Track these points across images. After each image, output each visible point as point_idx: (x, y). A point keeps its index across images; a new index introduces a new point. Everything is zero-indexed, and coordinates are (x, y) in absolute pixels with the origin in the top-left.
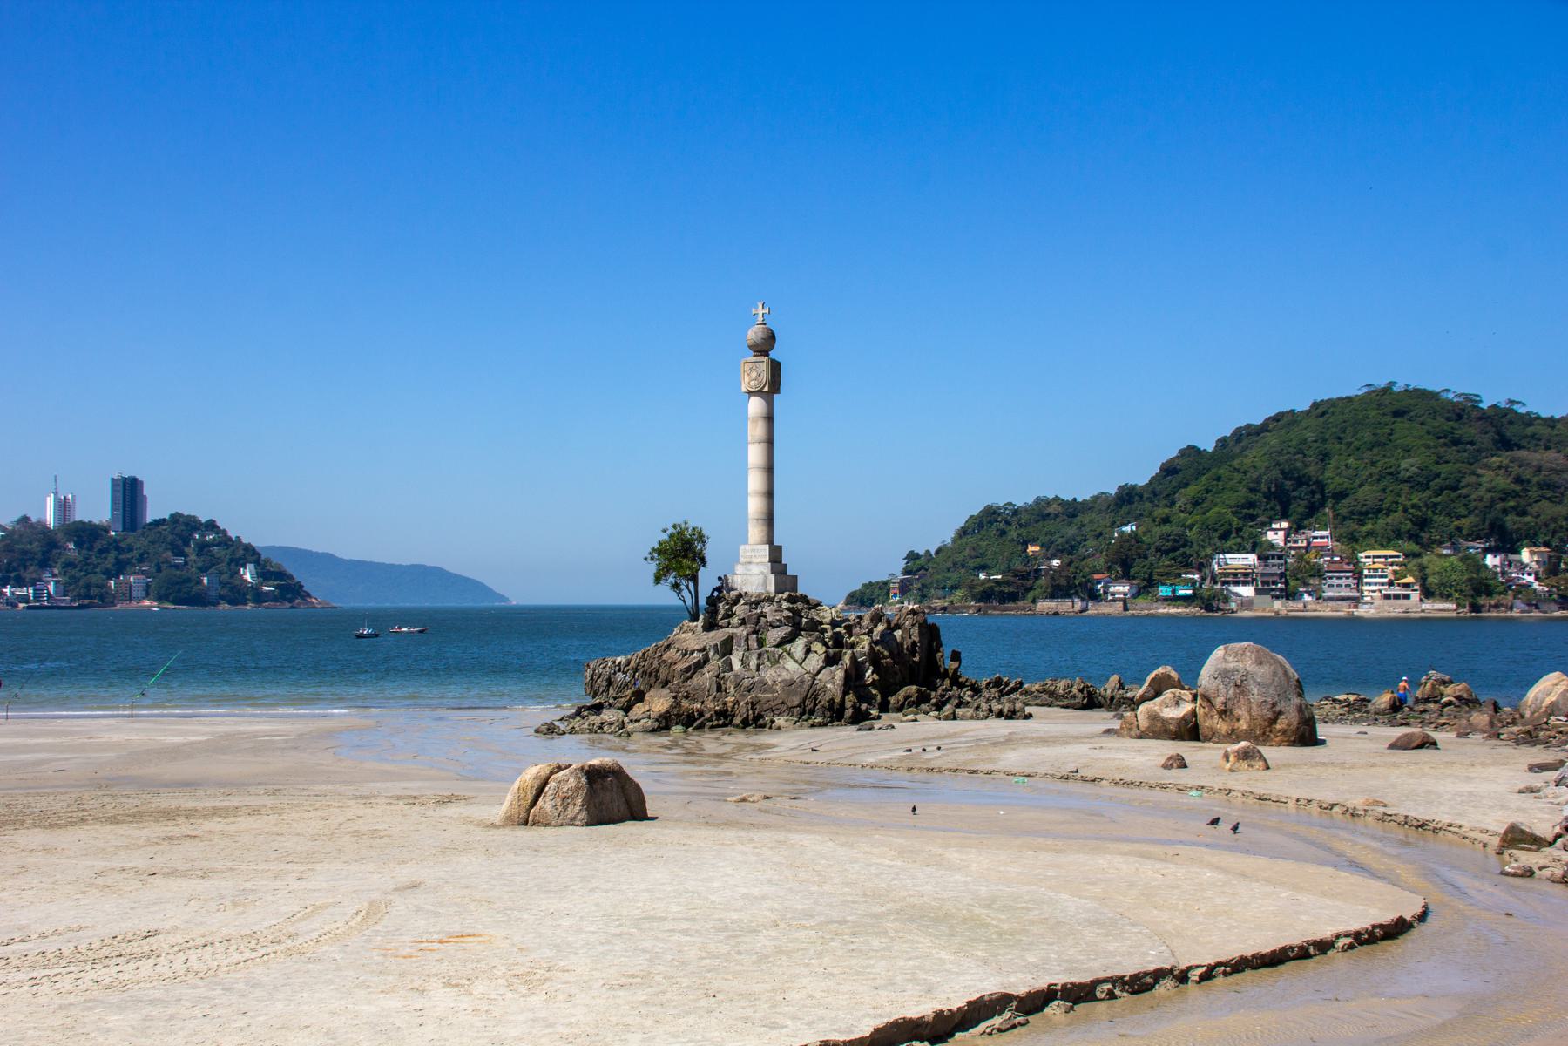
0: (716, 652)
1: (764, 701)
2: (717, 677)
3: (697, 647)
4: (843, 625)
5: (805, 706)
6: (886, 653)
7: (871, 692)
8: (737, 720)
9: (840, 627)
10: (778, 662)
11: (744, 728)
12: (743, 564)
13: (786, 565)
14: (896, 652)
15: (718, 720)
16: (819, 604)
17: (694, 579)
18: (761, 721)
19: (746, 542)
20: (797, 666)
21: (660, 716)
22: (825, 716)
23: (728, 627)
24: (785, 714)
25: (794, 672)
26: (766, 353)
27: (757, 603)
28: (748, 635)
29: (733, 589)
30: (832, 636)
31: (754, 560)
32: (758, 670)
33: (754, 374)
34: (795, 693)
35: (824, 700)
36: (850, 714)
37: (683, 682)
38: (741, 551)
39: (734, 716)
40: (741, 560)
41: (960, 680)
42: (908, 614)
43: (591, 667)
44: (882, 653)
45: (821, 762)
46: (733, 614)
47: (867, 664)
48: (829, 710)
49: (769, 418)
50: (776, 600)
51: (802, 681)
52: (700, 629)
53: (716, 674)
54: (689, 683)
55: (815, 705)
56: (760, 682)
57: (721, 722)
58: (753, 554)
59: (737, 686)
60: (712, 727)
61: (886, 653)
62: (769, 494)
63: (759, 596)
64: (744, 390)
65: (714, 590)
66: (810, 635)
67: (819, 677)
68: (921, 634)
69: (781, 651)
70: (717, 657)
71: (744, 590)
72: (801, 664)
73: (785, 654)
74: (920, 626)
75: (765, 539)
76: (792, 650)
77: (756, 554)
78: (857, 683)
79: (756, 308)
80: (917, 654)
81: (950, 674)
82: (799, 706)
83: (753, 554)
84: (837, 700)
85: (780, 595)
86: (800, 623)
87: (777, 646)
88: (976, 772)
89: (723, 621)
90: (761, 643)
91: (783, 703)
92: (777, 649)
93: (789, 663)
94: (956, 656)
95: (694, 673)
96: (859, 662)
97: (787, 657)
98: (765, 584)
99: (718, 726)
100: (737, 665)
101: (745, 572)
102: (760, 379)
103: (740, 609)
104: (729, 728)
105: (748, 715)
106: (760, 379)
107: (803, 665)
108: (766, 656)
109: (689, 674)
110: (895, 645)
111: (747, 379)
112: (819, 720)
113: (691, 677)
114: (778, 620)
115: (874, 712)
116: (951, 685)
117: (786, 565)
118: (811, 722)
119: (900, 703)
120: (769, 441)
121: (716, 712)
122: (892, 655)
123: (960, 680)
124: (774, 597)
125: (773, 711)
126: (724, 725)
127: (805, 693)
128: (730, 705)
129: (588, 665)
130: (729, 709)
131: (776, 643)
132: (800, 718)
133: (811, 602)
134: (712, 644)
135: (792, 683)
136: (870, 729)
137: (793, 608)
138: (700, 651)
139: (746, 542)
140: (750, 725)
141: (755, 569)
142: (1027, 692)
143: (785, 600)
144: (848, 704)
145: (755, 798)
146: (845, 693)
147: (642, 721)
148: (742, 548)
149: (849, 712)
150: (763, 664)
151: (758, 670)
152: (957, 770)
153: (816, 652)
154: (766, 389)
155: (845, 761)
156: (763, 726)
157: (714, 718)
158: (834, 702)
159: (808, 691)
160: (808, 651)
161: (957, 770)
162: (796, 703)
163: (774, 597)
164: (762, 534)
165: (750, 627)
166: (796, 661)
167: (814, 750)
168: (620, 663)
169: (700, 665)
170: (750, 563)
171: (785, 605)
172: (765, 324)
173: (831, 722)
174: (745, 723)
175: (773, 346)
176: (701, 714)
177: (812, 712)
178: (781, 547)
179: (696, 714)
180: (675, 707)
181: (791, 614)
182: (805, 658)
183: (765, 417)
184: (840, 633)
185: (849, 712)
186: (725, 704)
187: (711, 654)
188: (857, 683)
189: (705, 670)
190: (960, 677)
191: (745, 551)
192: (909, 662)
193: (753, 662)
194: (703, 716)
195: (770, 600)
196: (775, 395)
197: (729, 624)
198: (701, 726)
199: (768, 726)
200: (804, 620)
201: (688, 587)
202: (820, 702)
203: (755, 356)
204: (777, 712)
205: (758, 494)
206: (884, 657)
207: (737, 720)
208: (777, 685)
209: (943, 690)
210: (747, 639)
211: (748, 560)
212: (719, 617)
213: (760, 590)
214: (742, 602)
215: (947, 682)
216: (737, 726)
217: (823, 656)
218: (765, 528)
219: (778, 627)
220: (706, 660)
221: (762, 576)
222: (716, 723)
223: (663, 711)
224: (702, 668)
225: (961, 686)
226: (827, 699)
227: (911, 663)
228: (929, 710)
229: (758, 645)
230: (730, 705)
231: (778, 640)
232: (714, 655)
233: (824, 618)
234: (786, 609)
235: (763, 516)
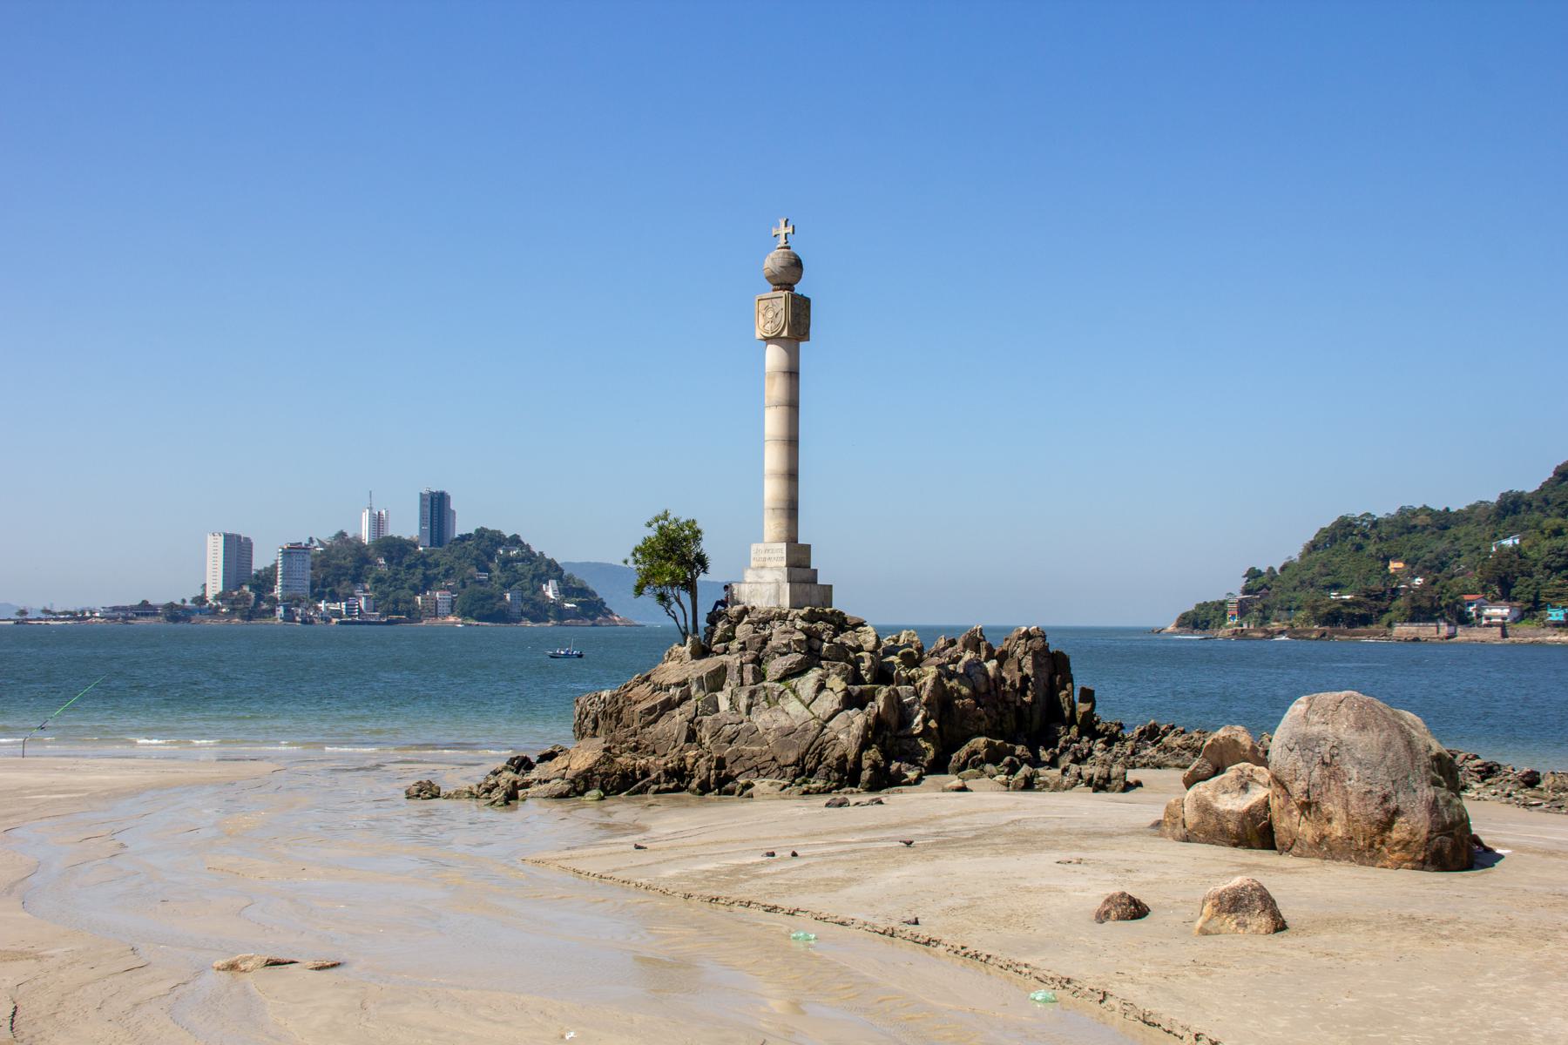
0: (701, 687)
1: (746, 757)
2: (691, 721)
3: (675, 680)
4: (900, 653)
5: (804, 766)
6: (965, 691)
7: (920, 746)
8: (694, 784)
9: (896, 655)
10: (777, 702)
11: (702, 794)
12: (753, 569)
13: (816, 571)
14: (983, 689)
15: (667, 782)
16: (862, 624)
17: (690, 586)
18: (730, 785)
19: (760, 539)
20: (802, 708)
21: (576, 776)
22: (829, 780)
23: (724, 653)
24: (775, 775)
25: (797, 717)
26: (789, 287)
27: (766, 621)
28: (742, 664)
29: (738, 603)
30: (870, 668)
31: (768, 564)
32: (749, 713)
33: (770, 315)
34: (792, 746)
35: (832, 756)
36: (867, 777)
37: (642, 728)
38: (752, 552)
39: (693, 777)
40: (753, 564)
41: (1098, 727)
42: (1019, 639)
43: (581, 702)
44: (958, 691)
45: (592, 873)
46: (733, 638)
47: (917, 707)
48: (837, 770)
49: (792, 374)
50: (790, 617)
51: (806, 730)
52: (688, 656)
53: (689, 717)
54: (651, 729)
55: (819, 762)
56: (748, 729)
57: (671, 786)
59: (716, 734)
60: (658, 792)
61: (965, 691)
62: (792, 475)
63: (769, 612)
64: (758, 336)
65: (718, 603)
66: (833, 666)
67: (831, 724)
68: (1036, 665)
69: (782, 687)
70: (701, 694)
71: (753, 604)
72: (808, 707)
73: (788, 691)
74: (1036, 655)
75: (784, 535)
76: (799, 686)
78: (901, 733)
79: (778, 227)
80: (1029, 693)
81: (1079, 720)
82: (796, 764)
83: (767, 555)
84: (851, 757)
85: (795, 611)
86: (820, 649)
87: (780, 680)
88: (774, 909)
89: (718, 646)
90: (760, 676)
91: (774, 759)
92: (778, 684)
93: (791, 704)
94: (1087, 695)
95: (661, 715)
96: (904, 704)
97: (791, 695)
98: (777, 595)
99: (668, 791)
100: (724, 704)
101: (756, 579)
102: (778, 320)
103: (743, 631)
104: (686, 794)
105: (709, 776)
106: (778, 320)
107: (811, 707)
108: (762, 694)
109: (652, 717)
110: (981, 679)
111: (761, 321)
112: (820, 784)
113: (655, 721)
114: (785, 645)
115: (912, 775)
116: (1080, 734)
117: (816, 571)
118: (805, 787)
119: (961, 761)
120: (792, 405)
121: (666, 772)
122: (975, 693)
123: (1098, 727)
124: (787, 614)
125: (758, 771)
126: (677, 789)
127: (807, 746)
128: (690, 761)
129: (577, 701)
130: (689, 767)
131: (778, 676)
132: (793, 781)
133: (849, 621)
134: (695, 676)
135: (792, 731)
136: (840, 805)
137: (809, 628)
138: (678, 685)
139: (760, 539)
140: (710, 791)
141: (769, 576)
142: (1166, 748)
143: (801, 617)
144: (866, 763)
145: (250, 964)
146: (865, 745)
147: (552, 782)
148: (754, 547)
149: (866, 774)
150: (757, 704)
151: (749, 713)
152: (749, 903)
153: (832, 689)
154: (785, 334)
155: (617, 875)
156: (731, 792)
157: (662, 779)
158: (846, 760)
159: (812, 744)
160: (821, 687)
161: (749, 903)
162: (792, 759)
163: (787, 614)
164: (778, 529)
165: (750, 655)
166: (802, 702)
167: (638, 847)
168: (605, 698)
169: (668, 705)
170: (763, 567)
171: (799, 624)
172: (789, 248)
173: (838, 788)
174: (704, 788)
175: (800, 278)
176: (646, 773)
177: (812, 772)
178: (810, 546)
179: (638, 772)
180: (604, 763)
181: (804, 637)
182: (816, 697)
184: (892, 662)
185: (866, 774)
186: (682, 759)
187: (694, 689)
188: (901, 733)
189: (677, 711)
190: (1098, 722)
191: (758, 551)
192: (1015, 702)
193: (743, 701)
194: (649, 776)
195: (782, 617)
196: (801, 343)
197: (727, 649)
198: (643, 790)
199: (737, 792)
200: (826, 645)
201: (678, 600)
202: (825, 759)
203: (774, 290)
204: (762, 772)
205: (775, 474)
206: (961, 697)
207: (694, 784)
208: (769, 734)
209: (1066, 742)
210: (741, 670)
211: (761, 563)
212: (714, 640)
213: (772, 604)
214: (746, 619)
215: (1074, 730)
216: (693, 791)
217: (840, 695)
218: (783, 521)
220: (686, 697)
221: (774, 586)
222: (664, 786)
223: (582, 769)
224: (673, 709)
225: (1095, 735)
226: (836, 755)
227: (1018, 704)
228: (995, 773)
229: (754, 679)
230: (690, 761)
231: (781, 671)
232: (698, 691)
233: (866, 643)
234: (800, 630)
235: (783, 505)
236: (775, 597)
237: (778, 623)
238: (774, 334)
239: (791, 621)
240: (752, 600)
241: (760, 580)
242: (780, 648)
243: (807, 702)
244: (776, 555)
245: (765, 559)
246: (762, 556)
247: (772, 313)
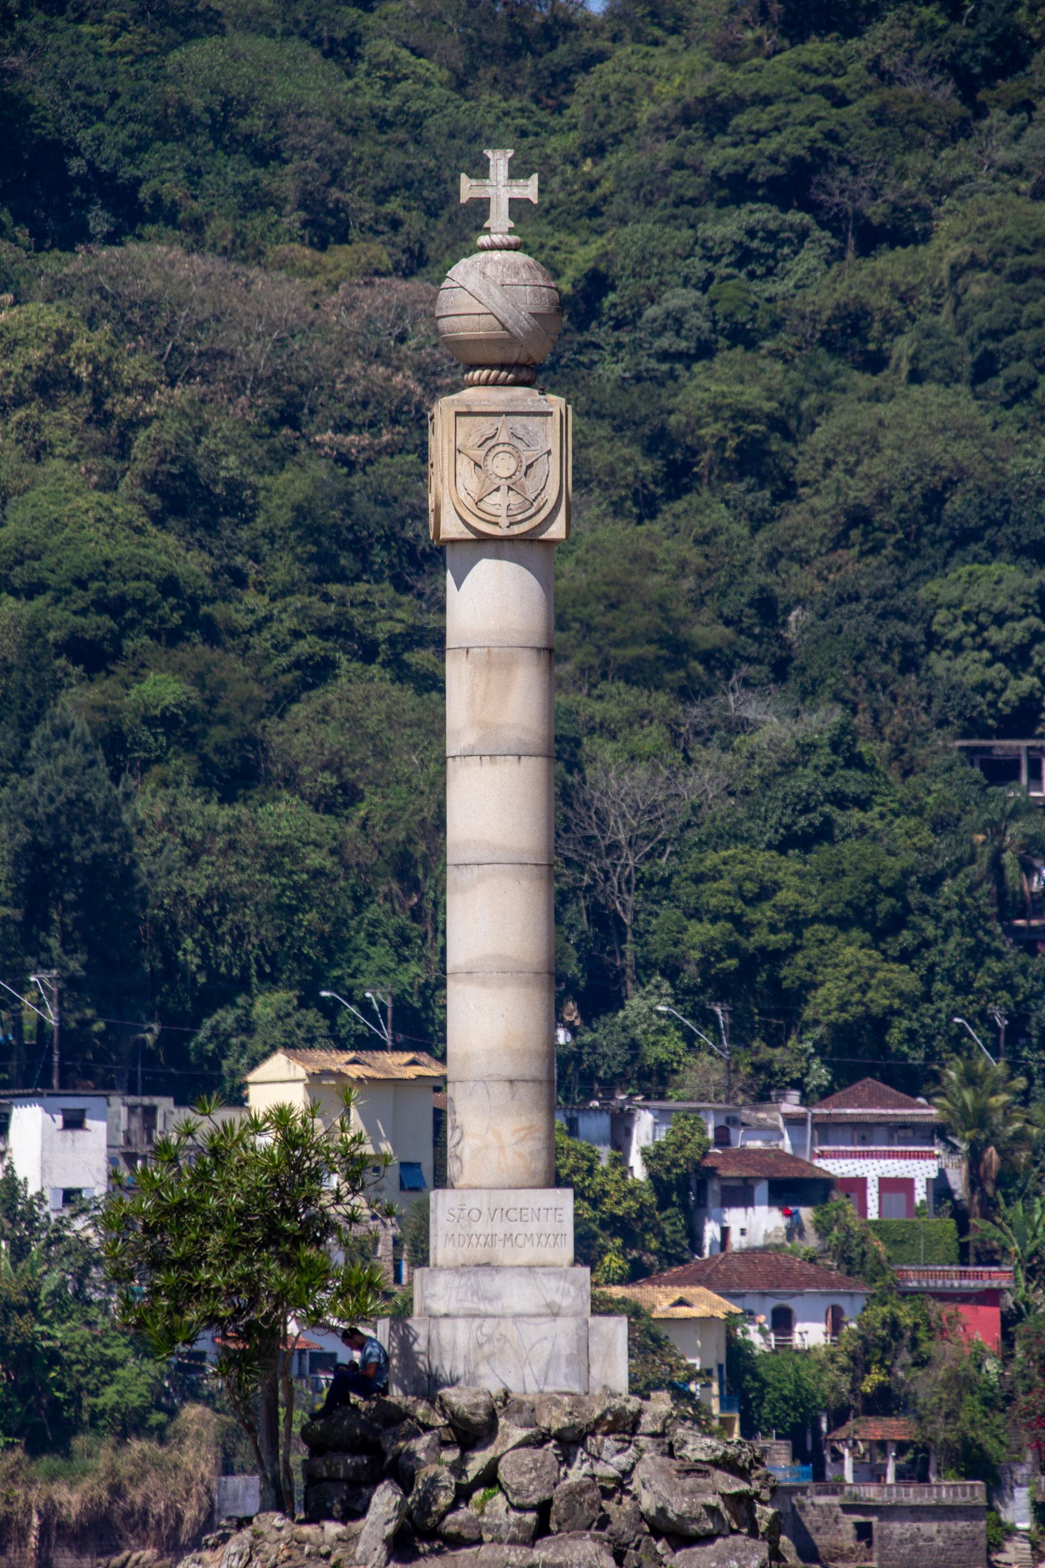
31: (504, 1254)
33: (503, 465)
58: (500, 1228)
77: (517, 1228)
83: (500, 1228)
101: (472, 1304)
102: (531, 488)
154: (557, 530)
183: (539, 650)
211: (479, 1253)
213: (562, 1381)
219: (708, 1538)
236: (571, 1360)
238: (517, 530)
239: (653, 1435)
240: (484, 1369)
241: (484, 1307)
242: (696, 1520)
244: (533, 1227)
245: (490, 1240)
246: (479, 1228)
247: (512, 464)
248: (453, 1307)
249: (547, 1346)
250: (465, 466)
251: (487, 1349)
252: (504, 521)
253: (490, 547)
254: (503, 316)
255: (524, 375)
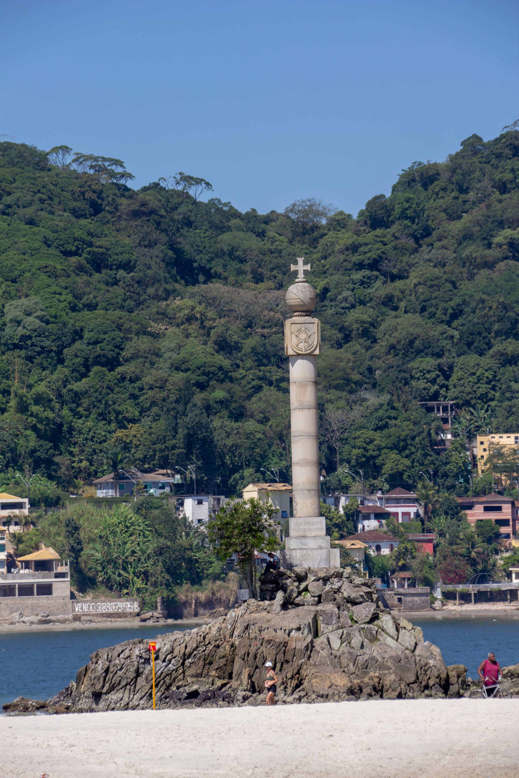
31: (308, 534)
33: (303, 336)
58: (307, 527)
77: (311, 527)
83: (307, 527)
98: (328, 559)
154: (317, 352)
166: (392, 637)
211: (302, 534)
213: (323, 565)
219: (361, 603)
236: (325, 560)
237: (336, 580)
238: (307, 352)
239: (347, 578)
240: (304, 562)
241: (304, 547)
242: (358, 598)
243: (396, 638)
244: (315, 527)
245: (305, 530)
246: (302, 527)
247: (305, 336)
248: (296, 547)
249: (320, 556)
250: (293, 337)
251: (304, 557)
252: (304, 350)
253: (300, 357)
254: (302, 299)
255: (308, 314)
